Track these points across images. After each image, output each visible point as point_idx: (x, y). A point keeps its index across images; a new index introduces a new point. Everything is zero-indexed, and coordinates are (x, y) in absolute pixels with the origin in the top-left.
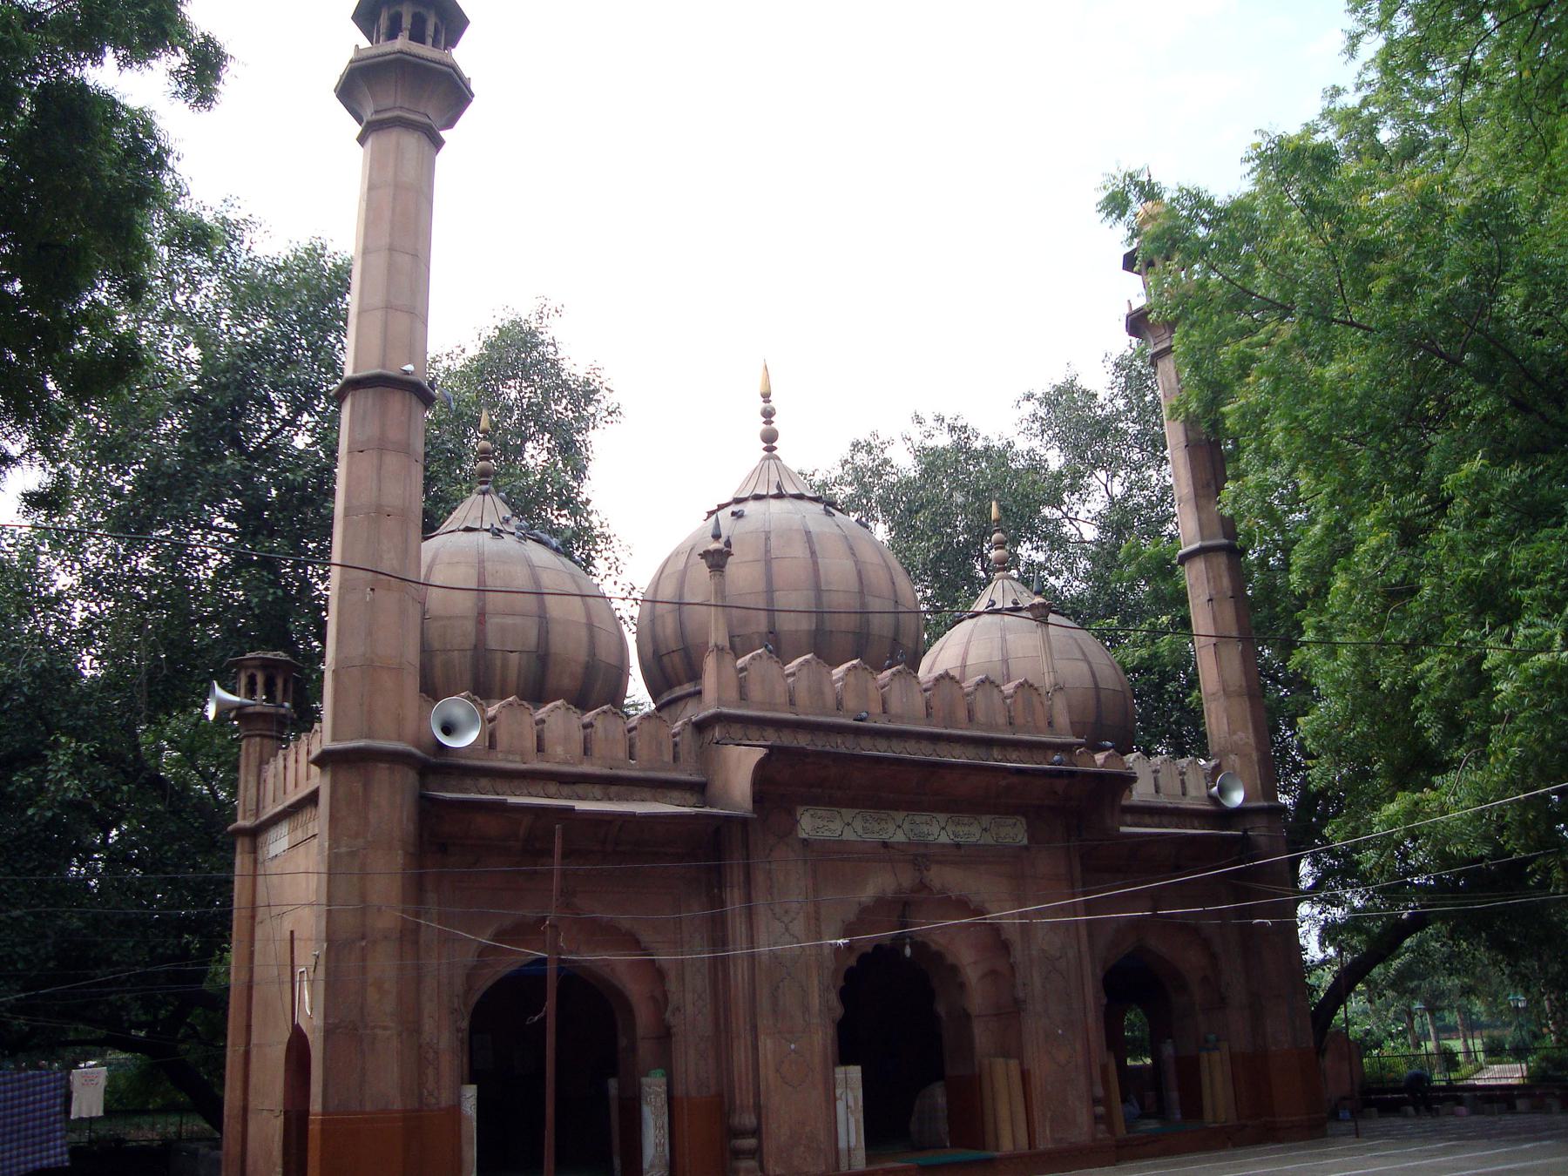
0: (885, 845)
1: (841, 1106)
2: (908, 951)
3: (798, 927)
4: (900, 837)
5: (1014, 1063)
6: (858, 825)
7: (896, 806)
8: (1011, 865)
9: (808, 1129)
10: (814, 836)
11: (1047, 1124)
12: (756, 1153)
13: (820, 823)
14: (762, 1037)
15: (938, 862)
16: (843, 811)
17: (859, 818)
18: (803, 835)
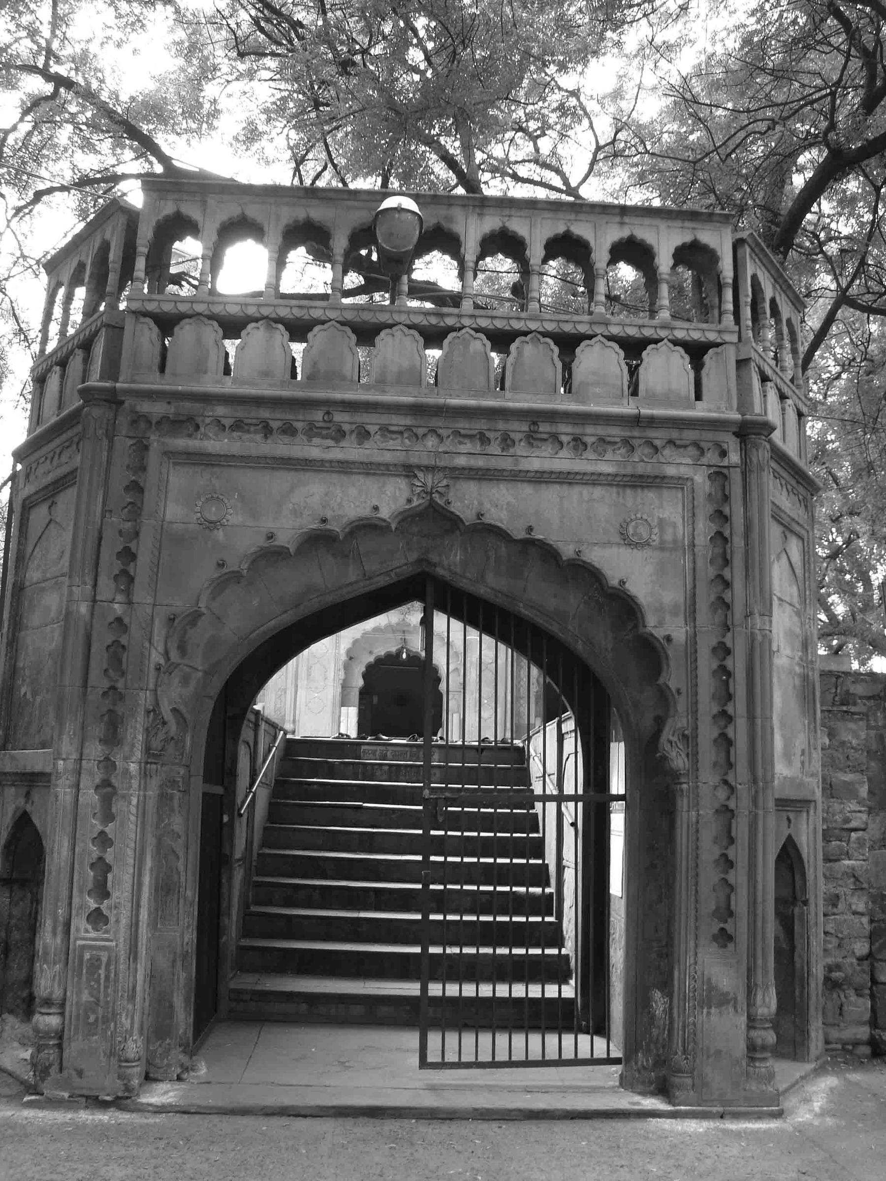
2: (404, 656)
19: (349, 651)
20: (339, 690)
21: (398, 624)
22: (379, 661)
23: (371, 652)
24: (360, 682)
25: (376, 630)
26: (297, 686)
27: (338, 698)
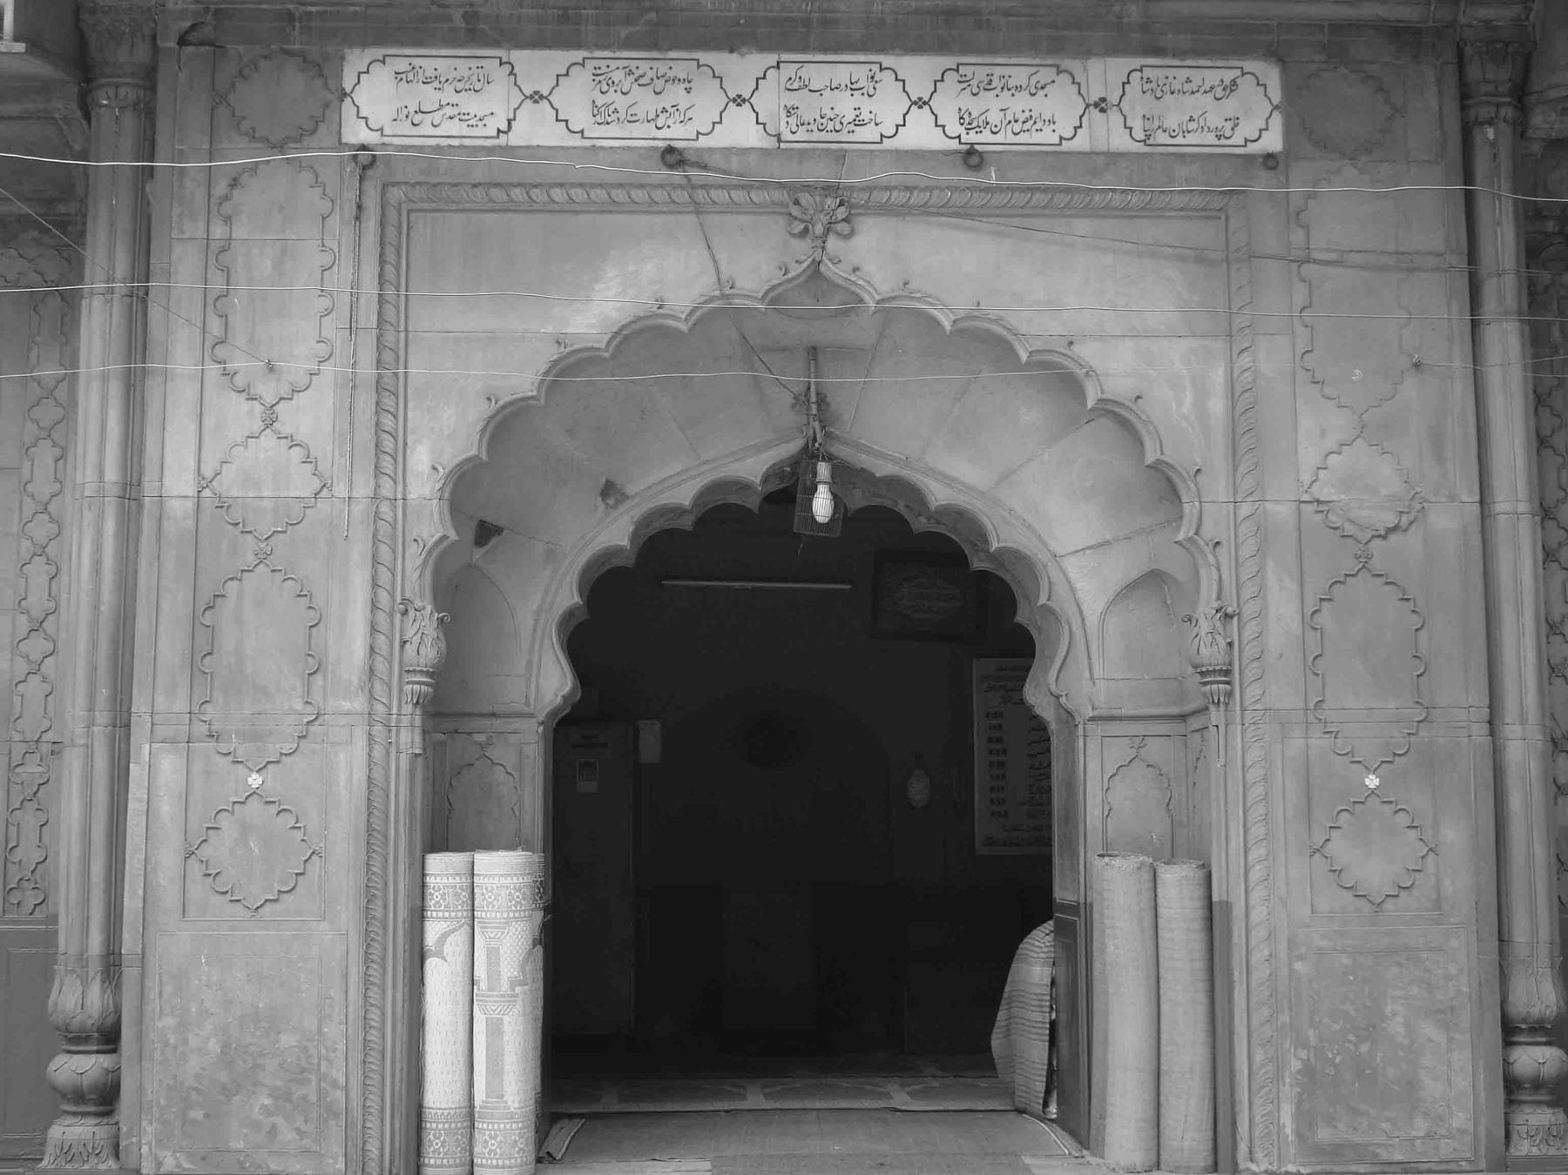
0: (672, 156)
1: (441, 979)
2: (822, 506)
3: (313, 415)
4: (740, 131)
5: (1177, 882)
6: (576, 98)
7: (733, 37)
8: (1210, 215)
9: (287, 1040)
10: (401, 134)
11: (1288, 1090)
12: (104, 1099)
13: (429, 96)
14: (142, 749)
15: (885, 210)
16: (519, 57)
17: (582, 77)
18: (356, 133)
19: (463, 486)
20: (409, 739)
21: (775, 297)
22: (666, 551)
23: (610, 491)
24: (552, 681)
25: (642, 338)
26: (122, 725)
27: (403, 794)
